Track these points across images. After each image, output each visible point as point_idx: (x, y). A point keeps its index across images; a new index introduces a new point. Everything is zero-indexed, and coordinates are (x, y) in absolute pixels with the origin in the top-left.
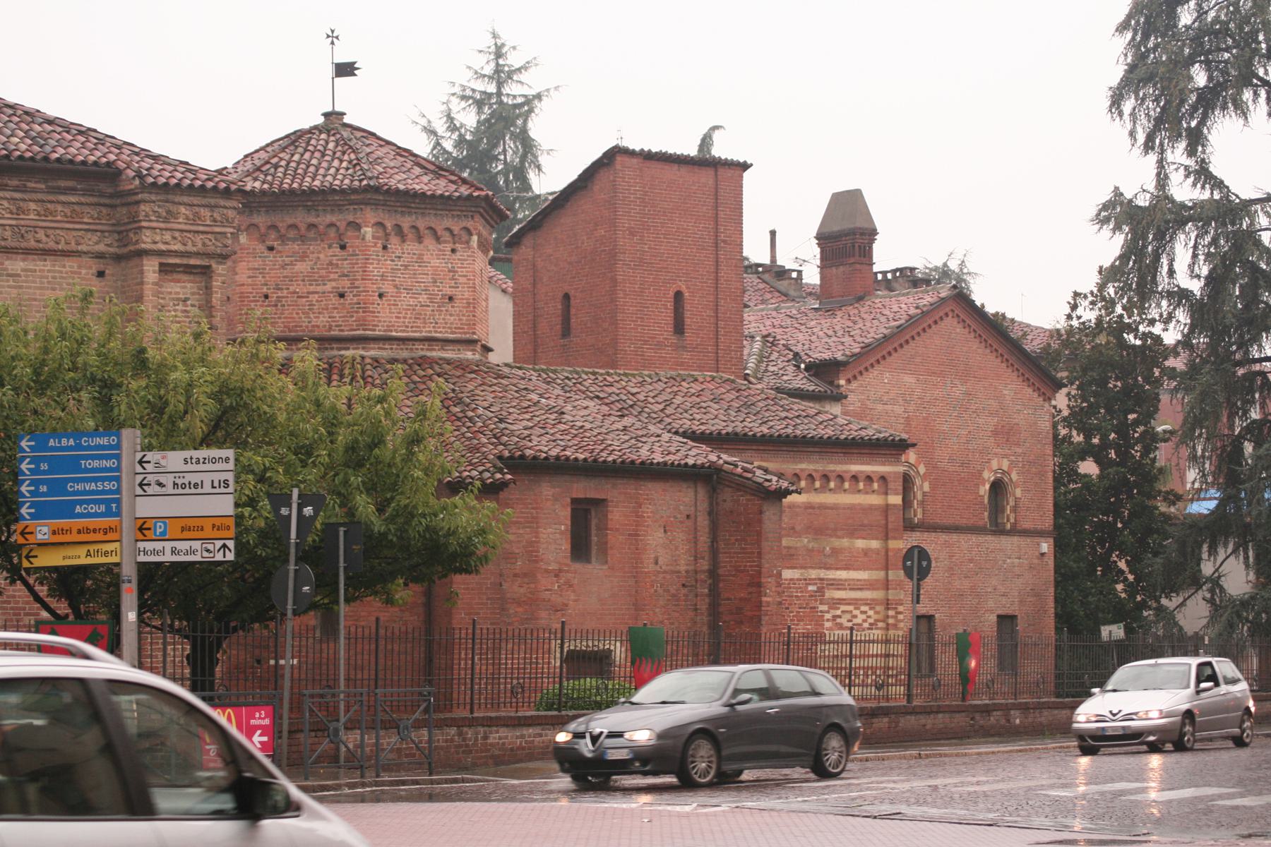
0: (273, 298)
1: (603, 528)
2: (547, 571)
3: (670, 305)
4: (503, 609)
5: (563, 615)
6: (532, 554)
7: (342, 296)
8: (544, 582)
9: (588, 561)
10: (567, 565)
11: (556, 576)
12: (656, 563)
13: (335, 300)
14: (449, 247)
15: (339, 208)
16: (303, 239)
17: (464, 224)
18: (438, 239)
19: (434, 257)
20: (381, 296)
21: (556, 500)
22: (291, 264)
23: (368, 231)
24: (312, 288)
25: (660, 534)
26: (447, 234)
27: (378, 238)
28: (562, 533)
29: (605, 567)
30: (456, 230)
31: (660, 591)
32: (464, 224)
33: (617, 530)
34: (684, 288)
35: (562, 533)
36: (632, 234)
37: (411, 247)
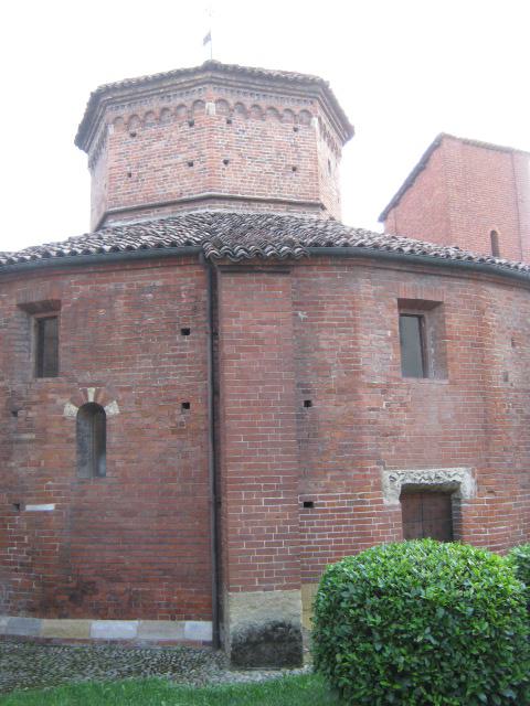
0: (135, 176)
1: (441, 336)
2: (371, 386)
3: (489, 239)
4: (315, 435)
5: (395, 440)
6: (350, 361)
7: (191, 165)
8: (368, 398)
9: (425, 376)
10: (399, 380)
11: (384, 392)
12: (506, 380)
13: (185, 169)
14: (291, 126)
15: (186, 90)
16: (159, 120)
17: (304, 107)
18: (280, 117)
19: (278, 132)
20: (226, 162)
21: (379, 300)
22: (150, 144)
23: (211, 107)
24: (166, 163)
25: (508, 346)
26: (290, 115)
27: (222, 113)
28: (388, 340)
29: (446, 382)
30: (297, 111)
31: (513, 411)
32: (304, 107)
33: (459, 338)
34: (497, 229)
35: (388, 340)
36: (458, 190)
37: (254, 124)
